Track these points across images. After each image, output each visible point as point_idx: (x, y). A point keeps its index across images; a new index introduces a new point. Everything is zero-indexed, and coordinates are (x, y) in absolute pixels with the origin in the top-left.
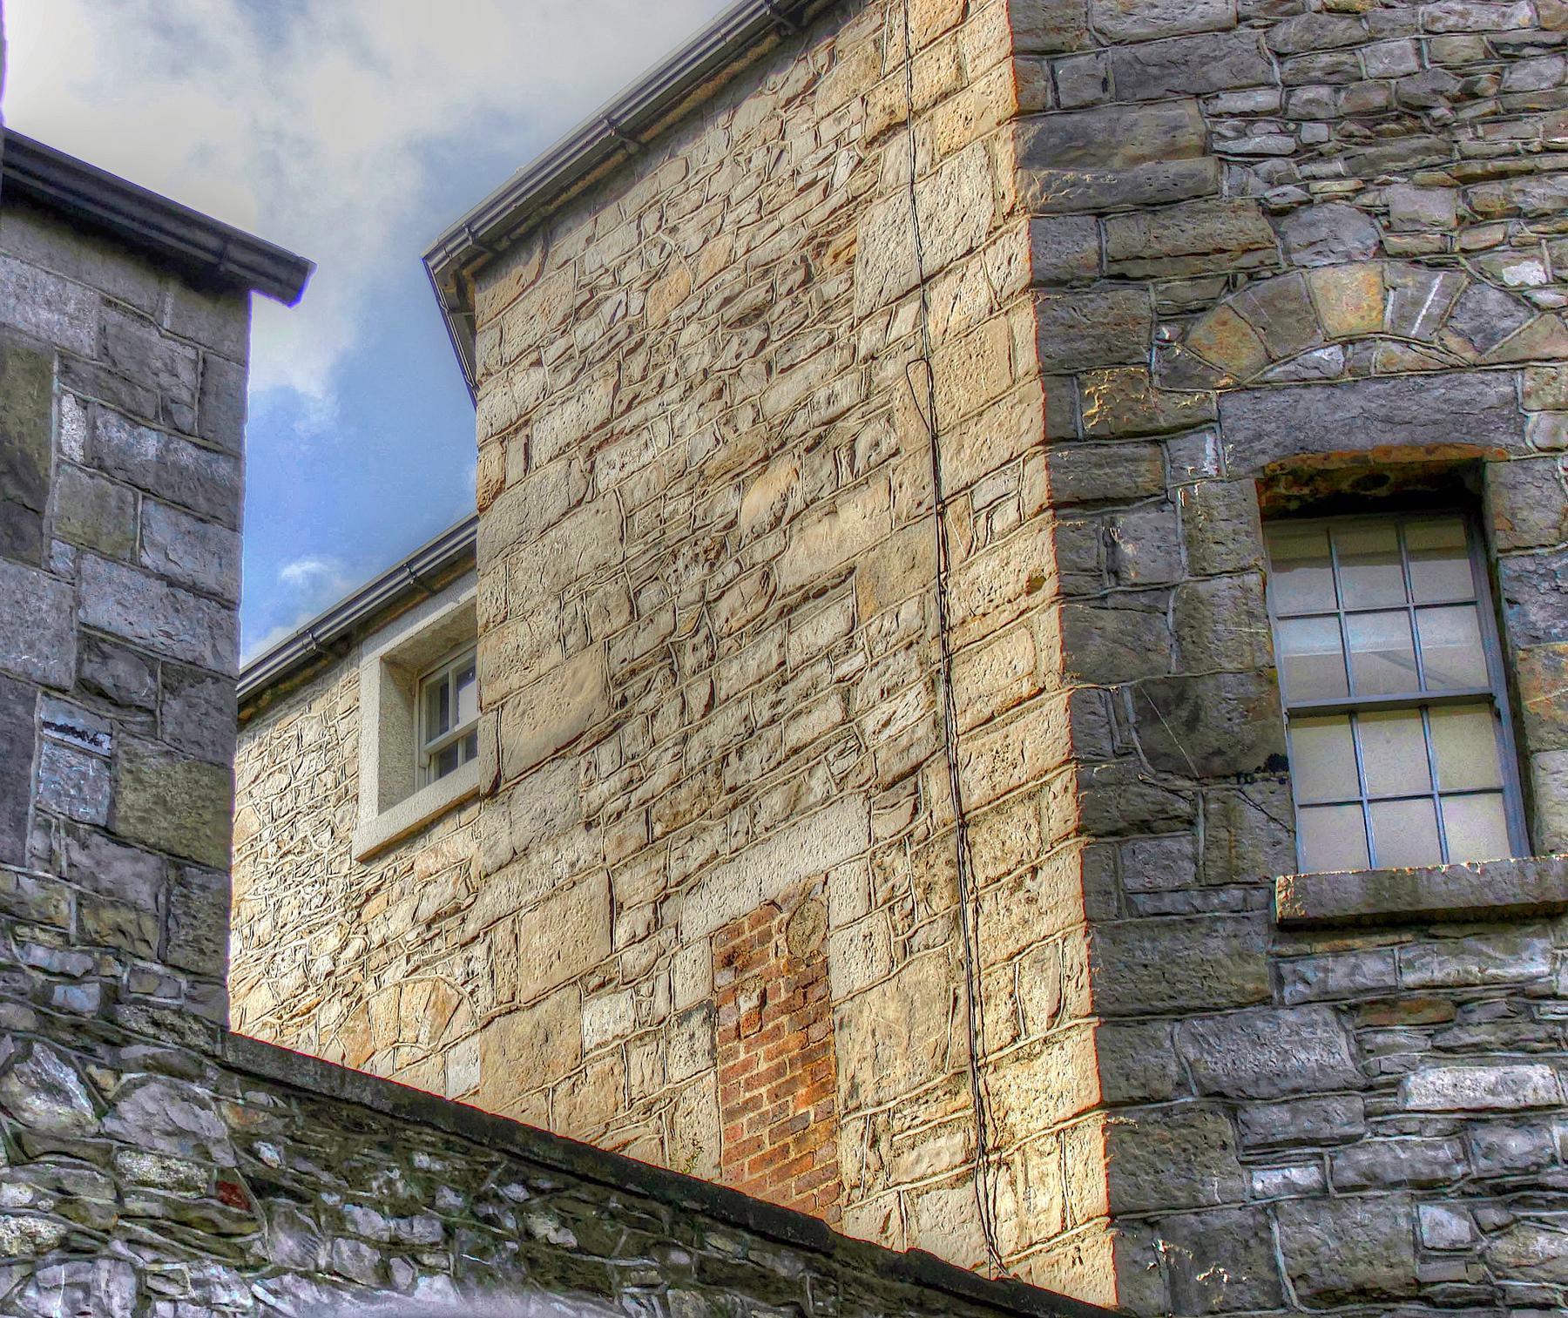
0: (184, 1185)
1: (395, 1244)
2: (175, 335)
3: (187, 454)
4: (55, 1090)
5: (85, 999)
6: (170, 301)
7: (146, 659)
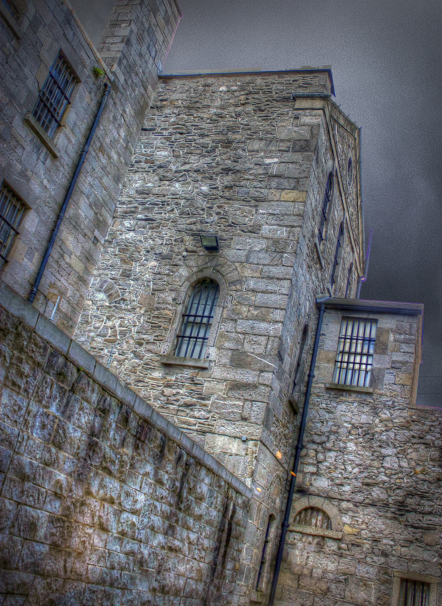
0: (402, 422)
1: (432, 425)
2: (406, 322)
3: (407, 336)
4: (385, 414)
6: (406, 319)
7: (401, 362)
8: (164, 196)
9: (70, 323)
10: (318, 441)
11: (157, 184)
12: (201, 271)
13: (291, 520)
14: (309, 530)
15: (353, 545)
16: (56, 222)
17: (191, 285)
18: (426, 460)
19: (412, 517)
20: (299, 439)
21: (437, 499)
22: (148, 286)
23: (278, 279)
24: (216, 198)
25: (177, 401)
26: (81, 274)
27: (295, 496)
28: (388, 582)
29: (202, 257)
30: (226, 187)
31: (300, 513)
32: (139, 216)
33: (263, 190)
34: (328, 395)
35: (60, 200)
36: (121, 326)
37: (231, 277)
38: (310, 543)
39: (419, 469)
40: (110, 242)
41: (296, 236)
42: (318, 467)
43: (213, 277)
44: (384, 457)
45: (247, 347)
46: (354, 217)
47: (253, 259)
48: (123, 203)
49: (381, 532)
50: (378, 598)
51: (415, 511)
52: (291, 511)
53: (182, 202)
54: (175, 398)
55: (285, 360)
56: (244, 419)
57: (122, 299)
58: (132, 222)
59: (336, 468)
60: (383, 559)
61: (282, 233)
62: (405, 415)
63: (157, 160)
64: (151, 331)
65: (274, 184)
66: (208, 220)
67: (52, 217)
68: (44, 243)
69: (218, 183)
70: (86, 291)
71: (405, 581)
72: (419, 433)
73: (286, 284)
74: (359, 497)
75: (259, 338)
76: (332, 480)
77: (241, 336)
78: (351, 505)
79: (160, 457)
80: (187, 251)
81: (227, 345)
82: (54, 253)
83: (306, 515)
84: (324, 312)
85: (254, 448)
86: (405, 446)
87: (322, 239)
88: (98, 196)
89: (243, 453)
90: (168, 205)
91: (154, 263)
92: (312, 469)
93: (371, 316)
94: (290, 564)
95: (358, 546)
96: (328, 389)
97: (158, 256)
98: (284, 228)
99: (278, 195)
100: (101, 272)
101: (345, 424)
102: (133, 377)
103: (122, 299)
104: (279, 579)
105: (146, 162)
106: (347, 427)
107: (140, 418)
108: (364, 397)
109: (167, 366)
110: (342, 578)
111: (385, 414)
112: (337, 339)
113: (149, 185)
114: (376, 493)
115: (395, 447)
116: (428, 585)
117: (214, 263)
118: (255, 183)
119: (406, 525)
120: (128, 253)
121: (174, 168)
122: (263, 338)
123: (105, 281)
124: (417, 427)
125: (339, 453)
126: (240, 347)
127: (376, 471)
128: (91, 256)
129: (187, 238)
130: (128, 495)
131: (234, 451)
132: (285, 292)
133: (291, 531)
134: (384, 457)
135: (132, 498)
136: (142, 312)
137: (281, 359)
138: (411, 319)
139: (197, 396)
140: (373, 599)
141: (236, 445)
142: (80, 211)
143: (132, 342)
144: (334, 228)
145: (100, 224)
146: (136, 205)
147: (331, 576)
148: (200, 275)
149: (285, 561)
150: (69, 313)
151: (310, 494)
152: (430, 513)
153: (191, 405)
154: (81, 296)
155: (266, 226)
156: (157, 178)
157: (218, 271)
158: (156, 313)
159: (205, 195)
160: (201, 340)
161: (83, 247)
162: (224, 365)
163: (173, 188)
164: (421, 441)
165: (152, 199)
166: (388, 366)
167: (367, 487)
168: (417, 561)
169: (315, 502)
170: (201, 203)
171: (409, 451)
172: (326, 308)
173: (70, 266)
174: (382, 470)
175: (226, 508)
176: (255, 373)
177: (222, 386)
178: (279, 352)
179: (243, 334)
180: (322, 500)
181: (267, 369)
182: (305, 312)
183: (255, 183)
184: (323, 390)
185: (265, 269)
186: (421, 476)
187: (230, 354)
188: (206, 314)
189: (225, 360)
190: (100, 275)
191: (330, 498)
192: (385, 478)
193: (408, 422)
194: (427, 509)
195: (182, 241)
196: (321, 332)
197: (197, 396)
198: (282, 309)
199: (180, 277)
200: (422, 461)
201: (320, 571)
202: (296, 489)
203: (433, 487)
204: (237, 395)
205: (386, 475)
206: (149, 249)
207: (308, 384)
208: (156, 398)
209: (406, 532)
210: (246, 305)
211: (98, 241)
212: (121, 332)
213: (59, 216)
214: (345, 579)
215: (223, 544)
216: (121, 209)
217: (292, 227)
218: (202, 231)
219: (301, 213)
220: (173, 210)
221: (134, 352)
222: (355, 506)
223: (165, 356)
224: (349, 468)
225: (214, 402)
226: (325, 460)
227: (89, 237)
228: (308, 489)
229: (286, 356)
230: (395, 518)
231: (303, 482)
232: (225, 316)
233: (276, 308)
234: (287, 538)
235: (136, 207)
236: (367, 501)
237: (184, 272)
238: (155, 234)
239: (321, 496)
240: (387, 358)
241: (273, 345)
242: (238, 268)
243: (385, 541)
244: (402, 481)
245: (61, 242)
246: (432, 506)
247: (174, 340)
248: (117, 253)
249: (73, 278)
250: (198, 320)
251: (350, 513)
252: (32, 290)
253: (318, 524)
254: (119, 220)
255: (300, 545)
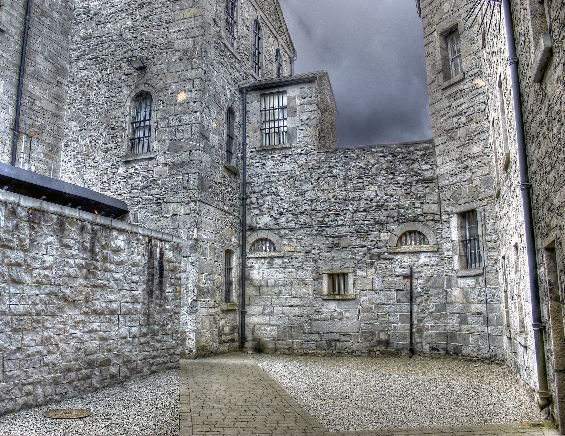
3: (310, 99)
4: (301, 160)
5: (304, 152)
6: (307, 86)
7: (307, 119)
8: (102, 36)
9: (56, 149)
10: (258, 191)
11: (95, 28)
12: (137, 87)
13: (248, 251)
14: (260, 255)
15: (292, 258)
16: (19, 80)
17: (132, 100)
18: (335, 188)
19: (330, 231)
20: (244, 192)
21: (346, 214)
22: (104, 108)
23: (191, 79)
24: (139, 29)
25: (138, 186)
26: (54, 112)
27: (248, 233)
28: (319, 279)
29: (136, 77)
30: (144, 18)
31: (253, 244)
32: (88, 57)
33: (170, 14)
34: (259, 156)
35: (18, 62)
36: (91, 142)
37: (158, 86)
38: (263, 264)
39: (330, 195)
40: (72, 82)
41: (200, 43)
42: (260, 210)
43: (146, 90)
44: (305, 192)
45: (178, 136)
46: (272, 12)
47: (172, 69)
48: (75, 50)
49: (310, 245)
50: (314, 291)
51: (331, 226)
52: (247, 244)
53: (115, 38)
54: (137, 184)
55: (211, 138)
56: (185, 188)
57: (88, 122)
58: (83, 63)
59: (273, 207)
60: (314, 264)
61: (189, 43)
62: (315, 158)
63: (92, 10)
64: (111, 140)
65: (177, 7)
66: (136, 47)
67: (16, 76)
68: (15, 97)
69: (138, 17)
70: (62, 123)
71: (331, 276)
72: (327, 169)
73: (198, 82)
74: (292, 225)
75: (186, 126)
76: (271, 217)
77: (173, 129)
78: (287, 231)
79: (61, 230)
80: (125, 75)
81: (165, 137)
82: (25, 102)
83: (258, 246)
84: (246, 94)
85: (195, 207)
86: (319, 181)
87: (235, 39)
88: (51, 50)
89: (189, 212)
90: (106, 43)
91: (104, 90)
92: (256, 212)
93: (281, 90)
94: (252, 280)
95: (296, 258)
96: (258, 151)
97: (106, 84)
98: (190, 40)
99: (181, 15)
100: (70, 106)
101: (275, 175)
102: (106, 177)
103: (88, 122)
104: (246, 292)
105: (85, 13)
106: (276, 176)
107: (29, 209)
108: (285, 151)
109: (126, 163)
110: (288, 282)
111: (301, 160)
112: (259, 112)
113: (90, 31)
114: (304, 219)
115: (312, 184)
116: (347, 274)
117: (145, 79)
118: (164, 10)
119: (326, 237)
120: (86, 86)
121: (104, 13)
122: (188, 126)
123: (74, 112)
124: (325, 165)
125: (273, 196)
126: (173, 137)
127: (301, 204)
128: (59, 96)
129: (123, 65)
130: (34, 259)
131: (182, 212)
132: (198, 88)
133: (249, 258)
134: (305, 192)
135: (40, 260)
136: (103, 128)
137: (207, 139)
138: (310, 85)
139: (151, 179)
140: (311, 292)
141: (182, 208)
142: (38, 66)
143: (100, 151)
144: (247, 27)
145: (59, 71)
146: (84, 49)
147: (281, 283)
148: (137, 91)
149: (249, 279)
150: (53, 142)
151: (258, 230)
152: (342, 225)
153: (148, 187)
154: (59, 127)
155: (177, 41)
156: (94, 24)
157: (149, 84)
158: (112, 126)
159: (130, 28)
160: (142, 139)
161: (49, 92)
162: (165, 153)
163: (107, 29)
164: (330, 175)
165: (93, 41)
166: (299, 125)
167: (296, 216)
168: (337, 260)
169: (262, 234)
170: (128, 35)
171: (322, 184)
172: (247, 91)
173: (43, 108)
174: (305, 201)
175: (151, 254)
176: (187, 153)
177: (165, 168)
178: (202, 134)
179: (174, 126)
180: (266, 232)
181: (194, 149)
182: (226, 98)
183: (164, 10)
184: (255, 153)
185: (182, 74)
186: (333, 201)
187: (167, 144)
188: (147, 118)
189: (165, 149)
190: (69, 109)
191: (271, 229)
192: (308, 207)
193: (318, 163)
194: (340, 222)
195: (120, 68)
196: (247, 110)
197: (151, 179)
198: (197, 102)
199: (124, 94)
200: (332, 189)
201: (273, 281)
202: (247, 228)
203: (342, 206)
204: (177, 172)
205: (308, 205)
206: (99, 80)
207: (244, 151)
208: (124, 187)
209: (327, 242)
210: (172, 105)
211: (62, 83)
212: (92, 146)
213: (20, 74)
214: (291, 283)
215: (157, 277)
216: (74, 55)
217: (196, 37)
218: (133, 56)
219: (201, 25)
220: (110, 46)
221: (103, 159)
222: (290, 231)
223: (123, 156)
224: (282, 206)
225: (163, 181)
226: (264, 203)
227: (53, 83)
228: (256, 226)
229: (211, 135)
230: (319, 234)
231: (252, 222)
232: (159, 116)
233: (194, 102)
234: (247, 263)
235: (84, 51)
236: (297, 226)
237: (126, 91)
238: (101, 67)
239: (265, 230)
240: (297, 119)
241: (196, 129)
242: (163, 79)
243: (313, 251)
244: (320, 206)
245: (28, 93)
246: (343, 220)
247: (128, 143)
248: (78, 89)
249: (48, 116)
250: (142, 124)
251: (288, 237)
252: (14, 134)
253: (267, 249)
254: (74, 64)
255: (256, 266)
